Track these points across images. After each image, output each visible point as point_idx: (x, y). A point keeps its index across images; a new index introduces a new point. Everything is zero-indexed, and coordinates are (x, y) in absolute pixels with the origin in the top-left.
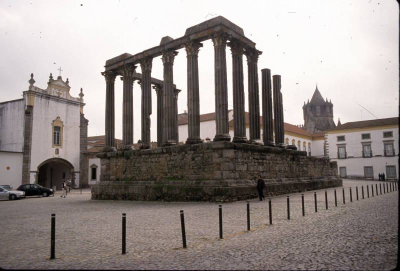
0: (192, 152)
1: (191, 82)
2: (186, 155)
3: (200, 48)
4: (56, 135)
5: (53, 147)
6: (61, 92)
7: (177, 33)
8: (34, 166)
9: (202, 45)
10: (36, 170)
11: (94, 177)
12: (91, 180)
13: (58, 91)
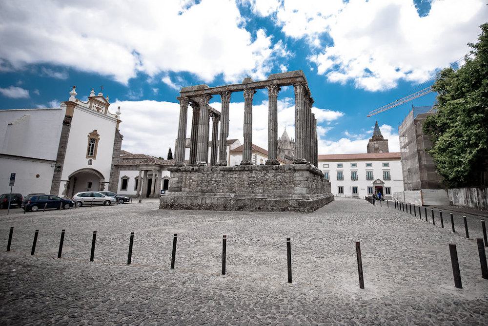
0: (274, 171)
4: (91, 147)
11: (124, 187)
12: (121, 190)
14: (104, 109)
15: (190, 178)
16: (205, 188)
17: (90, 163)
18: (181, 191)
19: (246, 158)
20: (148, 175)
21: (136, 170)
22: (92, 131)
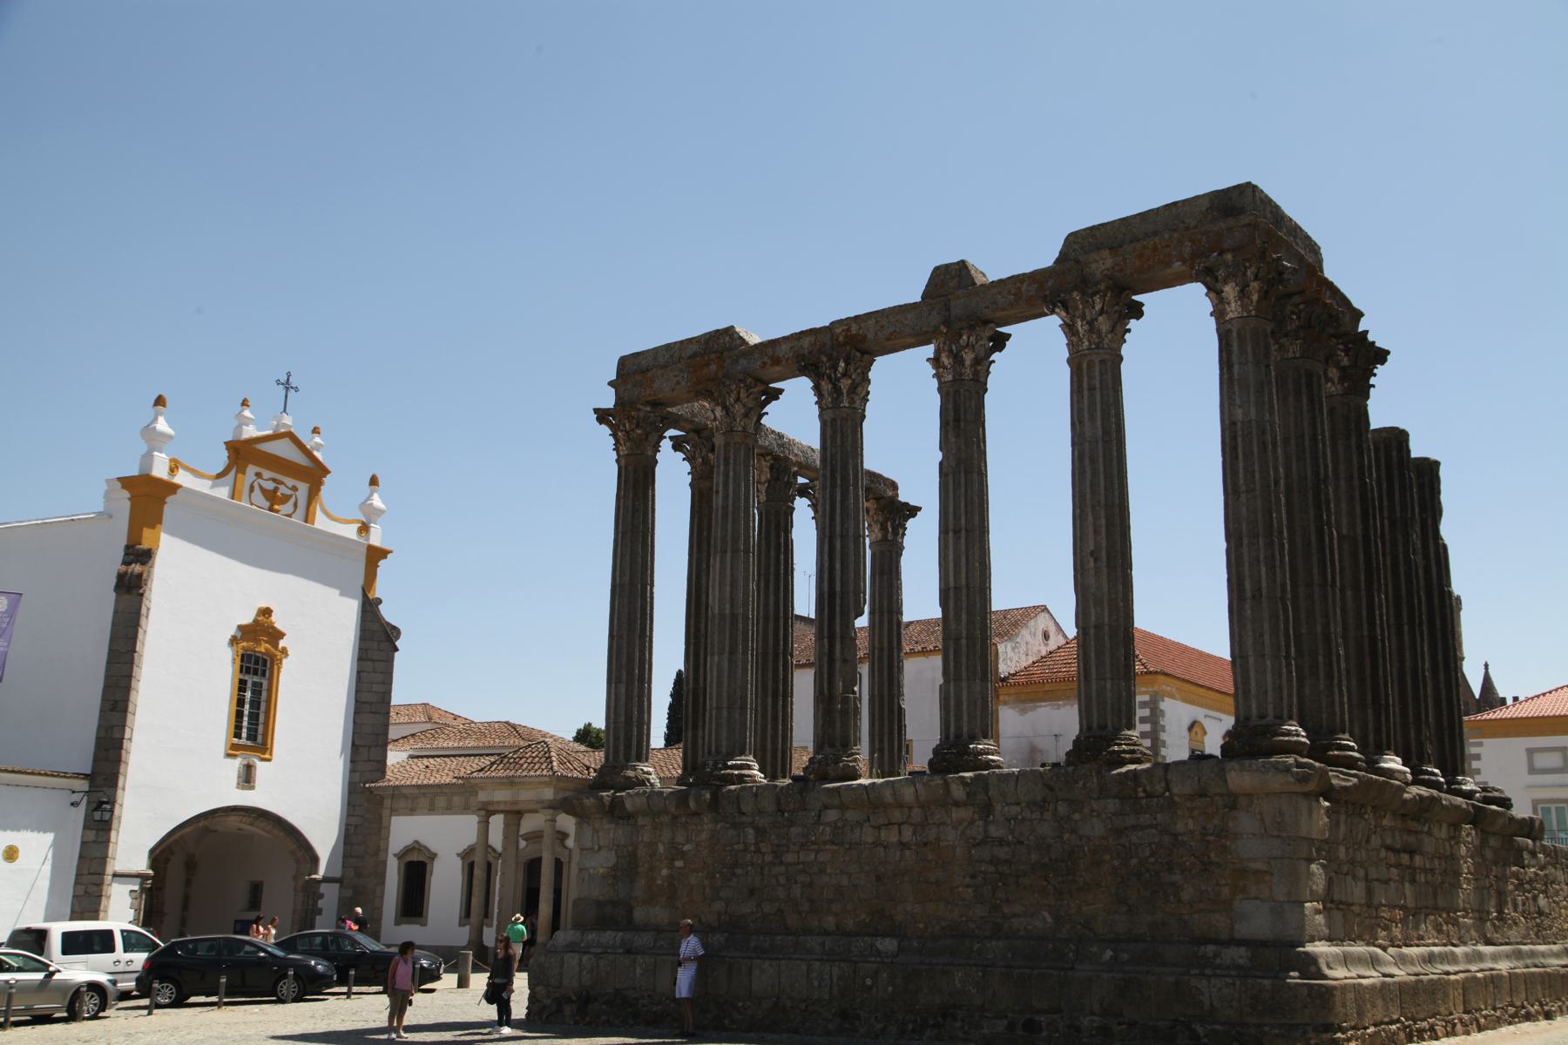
0: (1112, 805)
1: (1095, 473)
2: (1077, 816)
3: (1133, 324)
4: (248, 695)
5: (228, 755)
6: (283, 490)
7: (1016, 248)
8: (132, 848)
9: (1137, 311)
10: (141, 864)
11: (413, 903)
13: (270, 486)
14: (303, 488)
15: (675, 852)
16: (747, 908)
17: (247, 778)
18: (629, 925)
19: (959, 728)
20: (527, 837)
21: (466, 809)
22: (247, 618)
